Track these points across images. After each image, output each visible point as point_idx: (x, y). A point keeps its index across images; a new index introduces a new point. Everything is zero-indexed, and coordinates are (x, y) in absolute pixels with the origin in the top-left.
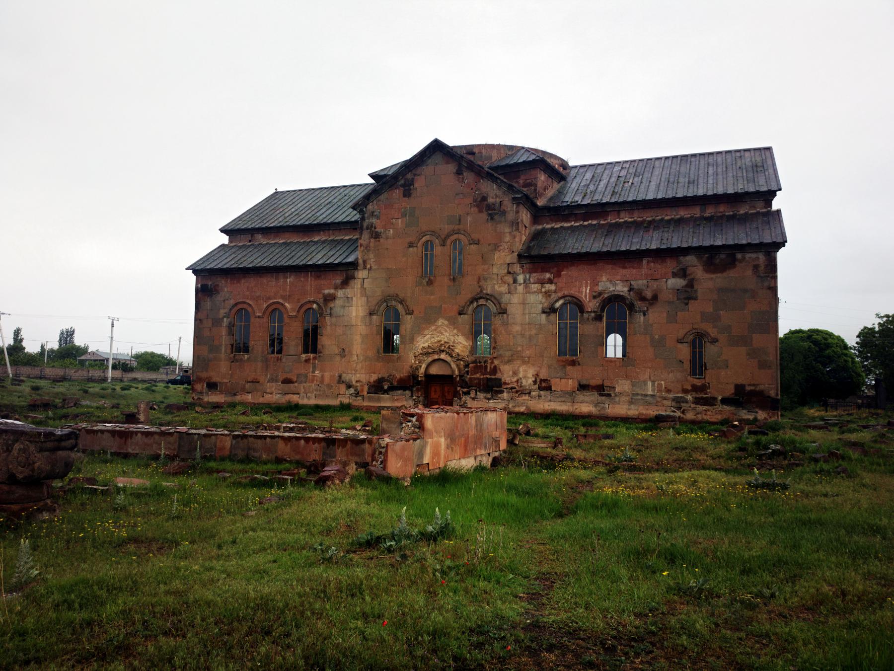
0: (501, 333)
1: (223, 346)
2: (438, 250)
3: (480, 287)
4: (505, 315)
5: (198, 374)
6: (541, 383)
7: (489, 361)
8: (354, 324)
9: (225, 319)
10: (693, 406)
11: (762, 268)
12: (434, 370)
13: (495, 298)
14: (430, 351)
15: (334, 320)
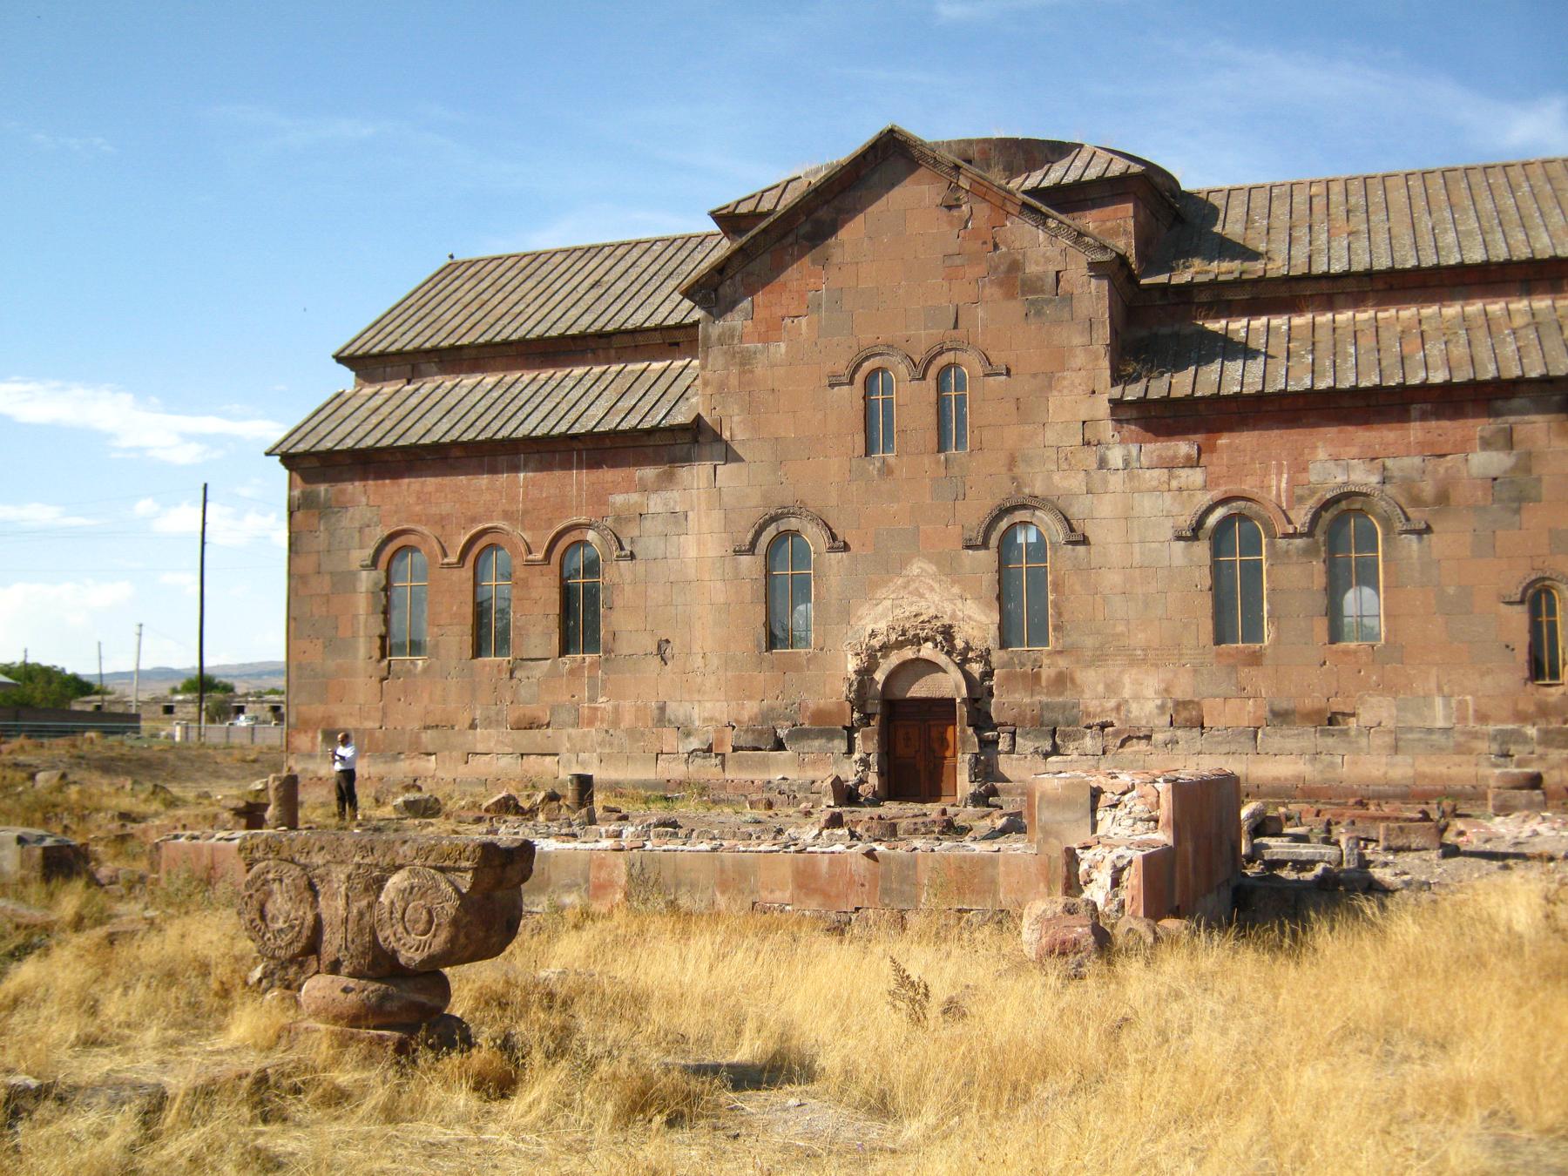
1: (362, 640)
3: (1014, 479)
4: (1081, 549)
5: (303, 709)
6: (1176, 711)
7: (1046, 661)
8: (692, 573)
10: (1539, 750)
15: (639, 566)
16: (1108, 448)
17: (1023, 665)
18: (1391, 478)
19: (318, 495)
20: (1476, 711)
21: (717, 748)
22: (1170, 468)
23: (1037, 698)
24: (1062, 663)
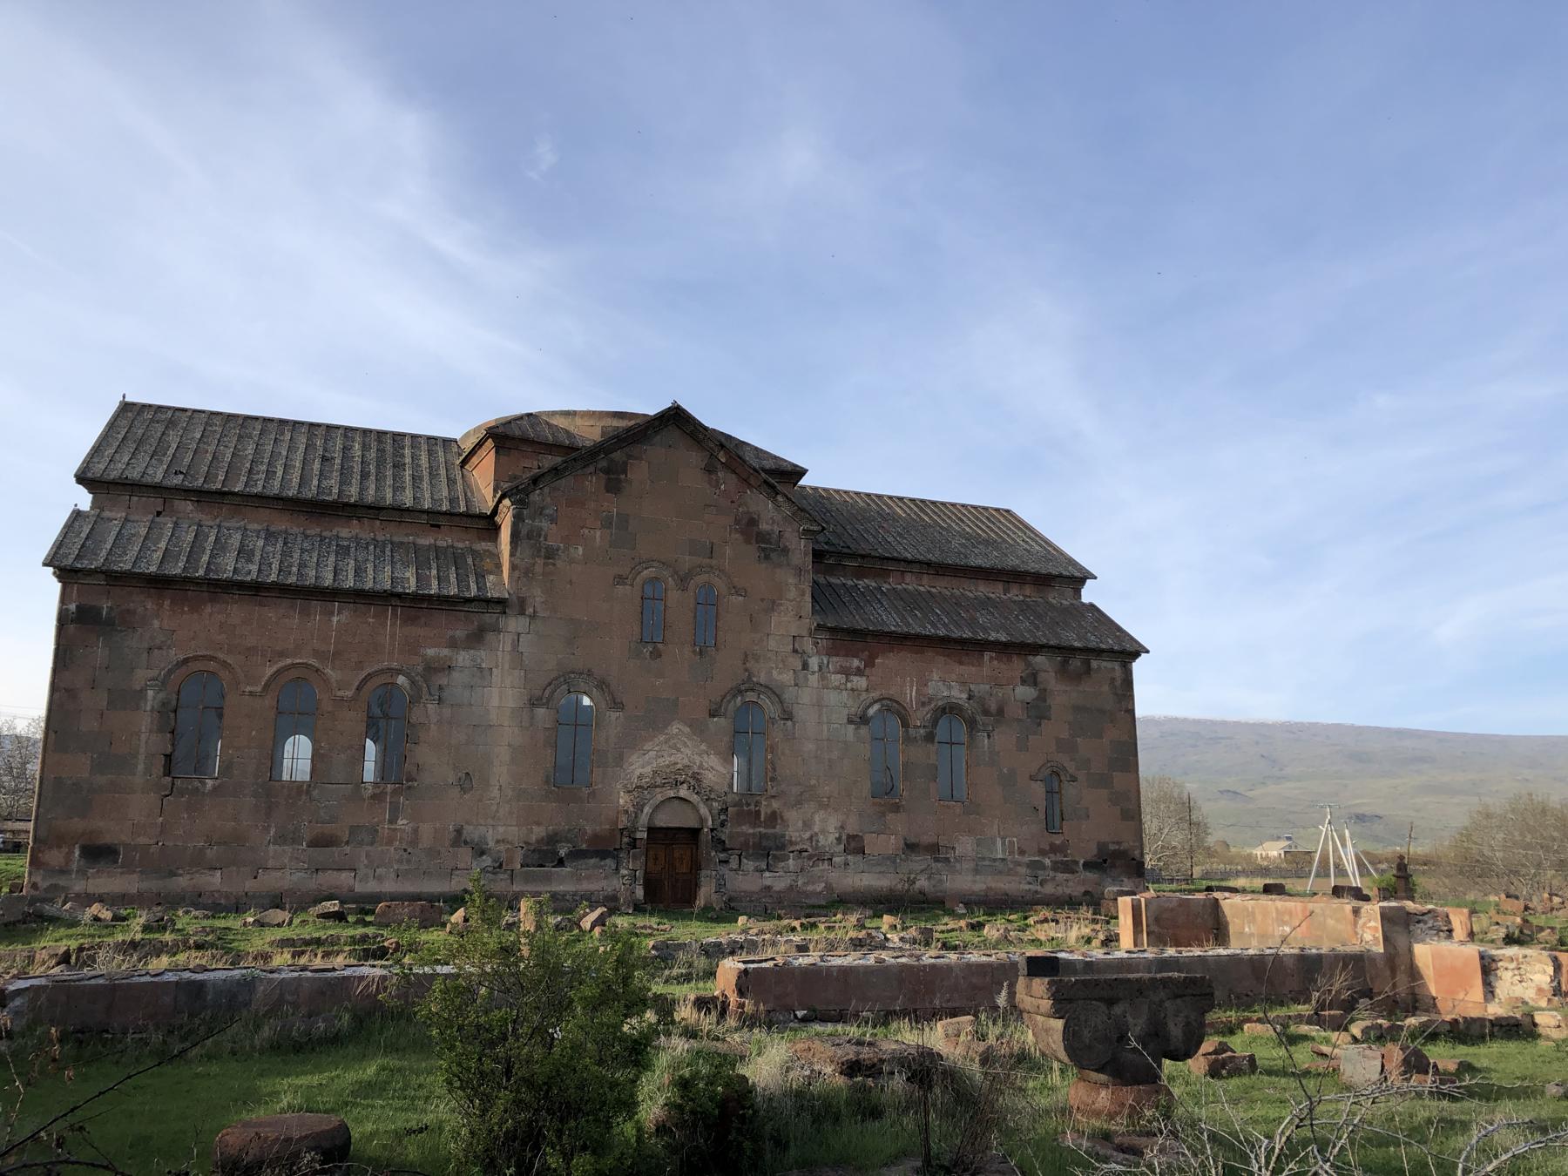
0: (783, 754)
1: (142, 757)
2: (674, 596)
3: (746, 670)
4: (789, 723)
6: (847, 841)
7: (764, 803)
9: (150, 693)
11: (1118, 683)
12: (663, 821)
13: (774, 693)
14: (659, 781)
15: (447, 712)
16: (809, 657)
17: (748, 805)
18: (974, 696)
19: (99, 610)
20: (1018, 848)
21: (507, 865)
22: (847, 675)
23: (758, 830)
24: (775, 805)
